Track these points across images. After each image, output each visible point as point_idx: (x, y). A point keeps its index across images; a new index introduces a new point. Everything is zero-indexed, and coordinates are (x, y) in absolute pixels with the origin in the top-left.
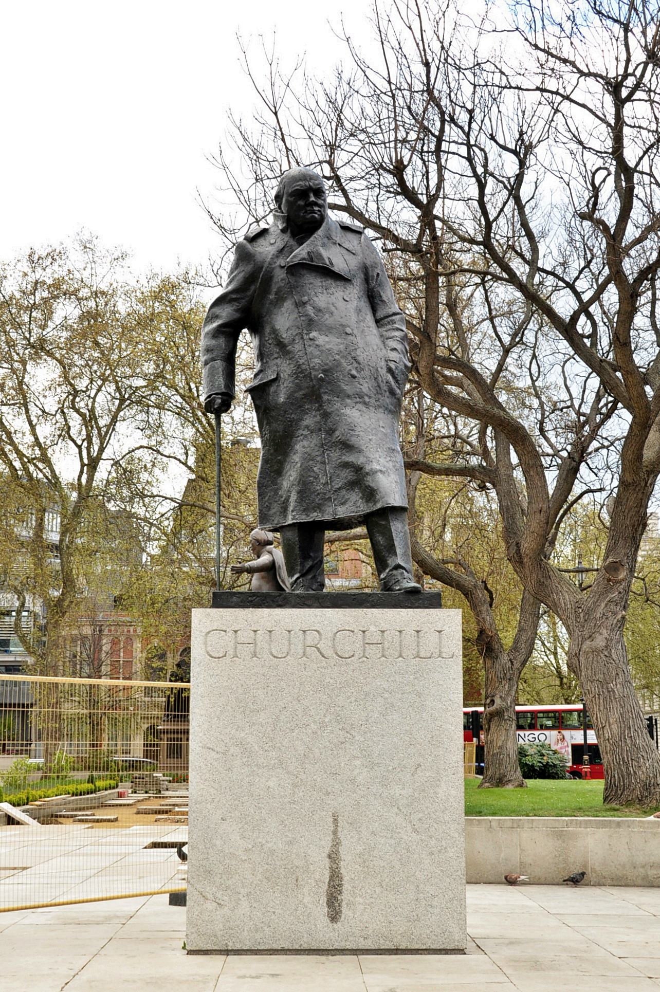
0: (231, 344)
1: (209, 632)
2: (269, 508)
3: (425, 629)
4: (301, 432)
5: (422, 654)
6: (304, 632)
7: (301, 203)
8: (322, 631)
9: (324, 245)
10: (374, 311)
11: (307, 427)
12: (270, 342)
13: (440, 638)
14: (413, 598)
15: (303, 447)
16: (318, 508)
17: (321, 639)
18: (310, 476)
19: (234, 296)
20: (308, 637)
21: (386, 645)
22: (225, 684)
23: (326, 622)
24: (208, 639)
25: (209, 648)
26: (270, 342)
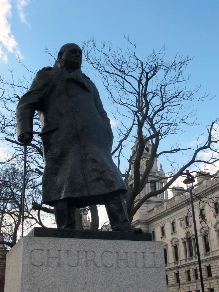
1: (33, 251)
5: (147, 266)
6: (86, 251)
7: (73, 55)
15: (71, 161)
17: (95, 257)
21: (129, 260)
24: (32, 254)
25: (33, 260)
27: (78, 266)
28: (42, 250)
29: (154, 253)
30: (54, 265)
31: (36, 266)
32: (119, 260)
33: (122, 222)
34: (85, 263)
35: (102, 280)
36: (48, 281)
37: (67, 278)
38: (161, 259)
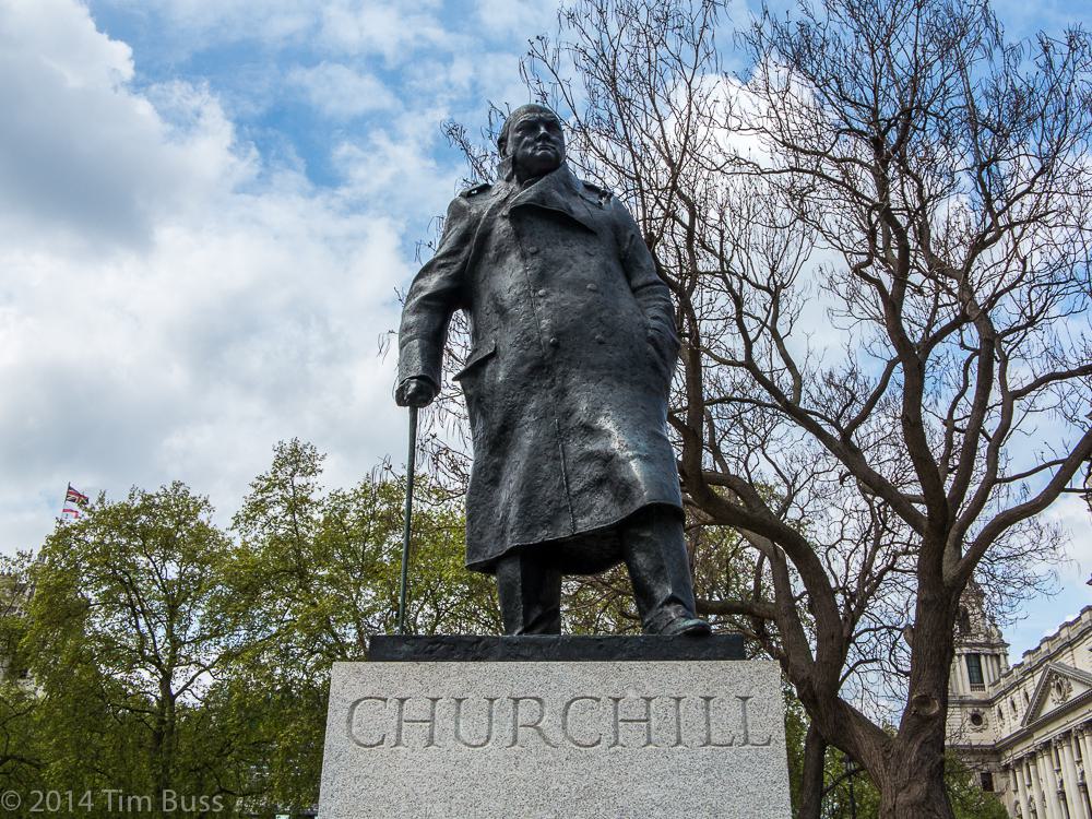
0: (438, 321)
2: (481, 535)
3: (721, 695)
4: (526, 418)
5: (715, 738)
6: (517, 700)
8: (546, 700)
9: (560, 191)
10: (629, 278)
11: (535, 411)
12: (488, 311)
13: (744, 710)
14: (699, 645)
15: (527, 437)
16: (549, 522)
17: (541, 716)
18: (537, 478)
19: (442, 262)
20: (520, 710)
22: (378, 793)
23: (553, 685)
26: (488, 311)
27: (489, 744)
28: (385, 700)
29: (747, 698)
30: (416, 743)
31: (365, 746)
32: (621, 724)
33: (662, 606)
34: (511, 735)
35: (562, 787)
36: (396, 789)
37: (453, 781)
38: (770, 716)
